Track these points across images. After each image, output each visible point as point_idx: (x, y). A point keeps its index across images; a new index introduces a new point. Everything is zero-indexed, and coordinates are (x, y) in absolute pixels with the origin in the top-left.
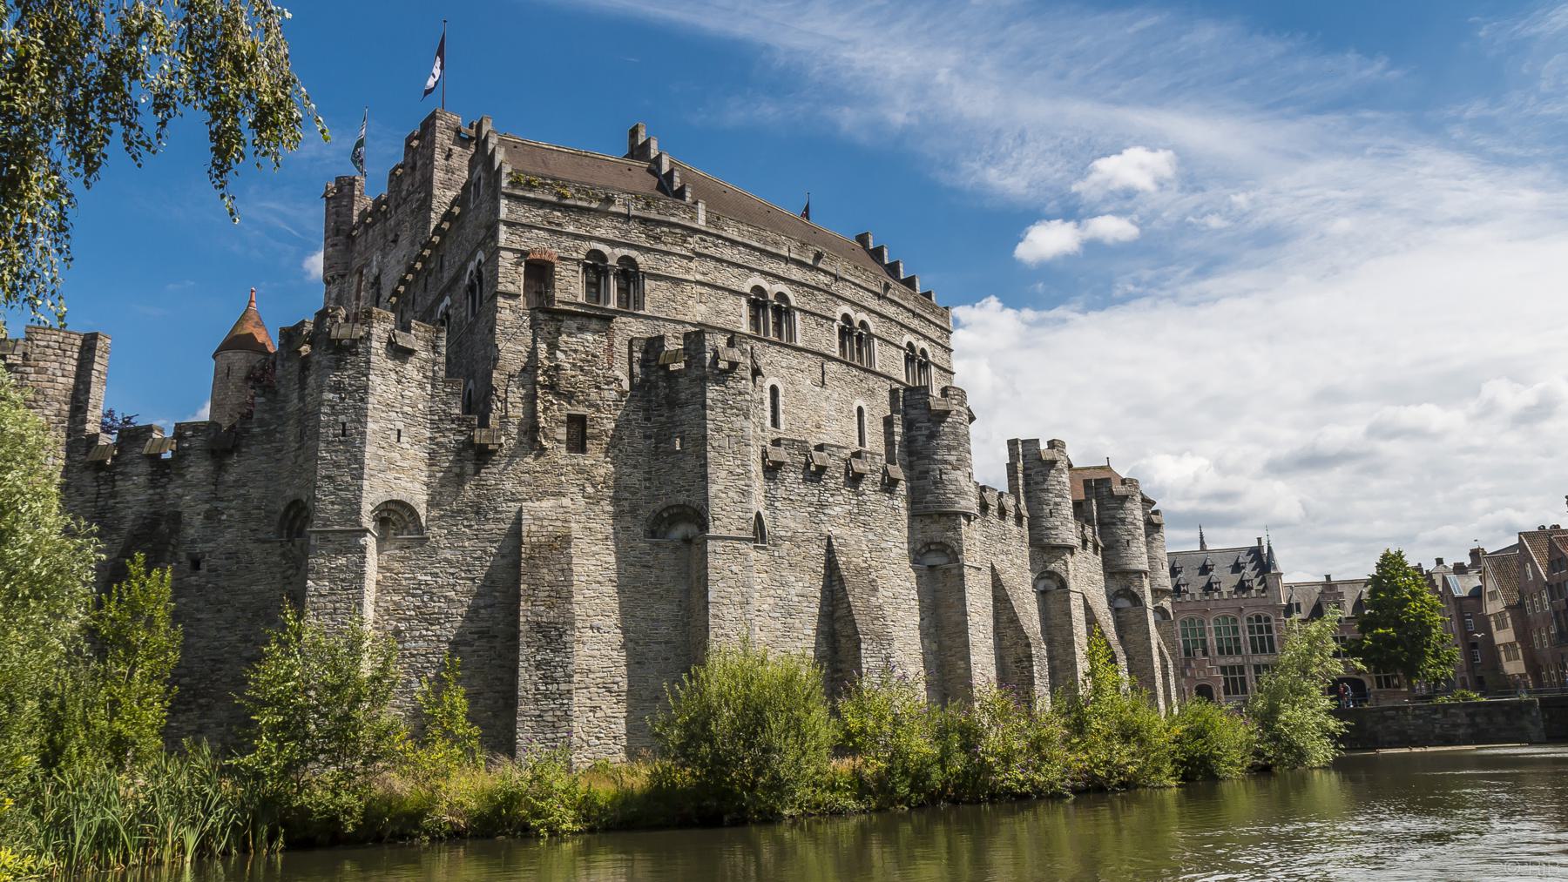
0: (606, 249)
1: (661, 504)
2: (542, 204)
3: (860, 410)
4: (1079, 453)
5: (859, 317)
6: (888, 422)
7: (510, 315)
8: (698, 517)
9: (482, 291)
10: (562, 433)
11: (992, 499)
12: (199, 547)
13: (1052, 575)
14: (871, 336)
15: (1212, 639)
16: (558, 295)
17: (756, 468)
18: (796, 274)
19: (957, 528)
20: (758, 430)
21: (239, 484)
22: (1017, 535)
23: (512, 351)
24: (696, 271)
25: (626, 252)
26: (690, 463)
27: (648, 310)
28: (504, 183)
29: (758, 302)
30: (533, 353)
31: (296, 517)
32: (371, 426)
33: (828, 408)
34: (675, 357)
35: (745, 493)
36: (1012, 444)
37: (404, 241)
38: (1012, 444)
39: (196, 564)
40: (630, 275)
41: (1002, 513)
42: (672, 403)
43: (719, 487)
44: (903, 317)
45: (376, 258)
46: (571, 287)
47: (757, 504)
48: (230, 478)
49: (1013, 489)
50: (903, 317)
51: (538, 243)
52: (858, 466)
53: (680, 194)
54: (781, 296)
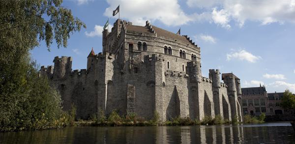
0: (141, 42)
1: (148, 81)
2: (132, 35)
3: (183, 65)
4: (223, 70)
5: (183, 50)
6: (186, 67)
7: (126, 52)
8: (154, 83)
9: (123, 48)
10: (134, 70)
11: (204, 79)
12: (84, 87)
13: (216, 91)
14: (185, 53)
15: (253, 103)
16: (134, 49)
17: (163, 75)
18: (172, 44)
19: (197, 84)
20: (163, 70)
21: (89, 78)
22: (210, 85)
23: (127, 58)
24: (156, 44)
25: (143, 42)
26: (153, 74)
27: (148, 50)
28: (126, 33)
29: (166, 48)
30: (129, 58)
31: (96, 83)
32: (106, 70)
33: (177, 65)
34: (151, 58)
35: (161, 79)
36: (210, 70)
37: (114, 40)
38: (210, 70)
39: (84, 89)
40: (145, 45)
41: (207, 81)
42: (151, 65)
43: (157, 77)
44: (192, 50)
45: (110, 42)
46: (136, 48)
47: (164, 80)
48: (88, 77)
49: (210, 78)
50: (192, 50)
51: (131, 41)
52: (181, 74)
53: (153, 32)
54: (169, 47)
